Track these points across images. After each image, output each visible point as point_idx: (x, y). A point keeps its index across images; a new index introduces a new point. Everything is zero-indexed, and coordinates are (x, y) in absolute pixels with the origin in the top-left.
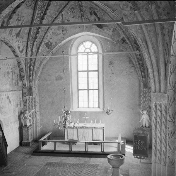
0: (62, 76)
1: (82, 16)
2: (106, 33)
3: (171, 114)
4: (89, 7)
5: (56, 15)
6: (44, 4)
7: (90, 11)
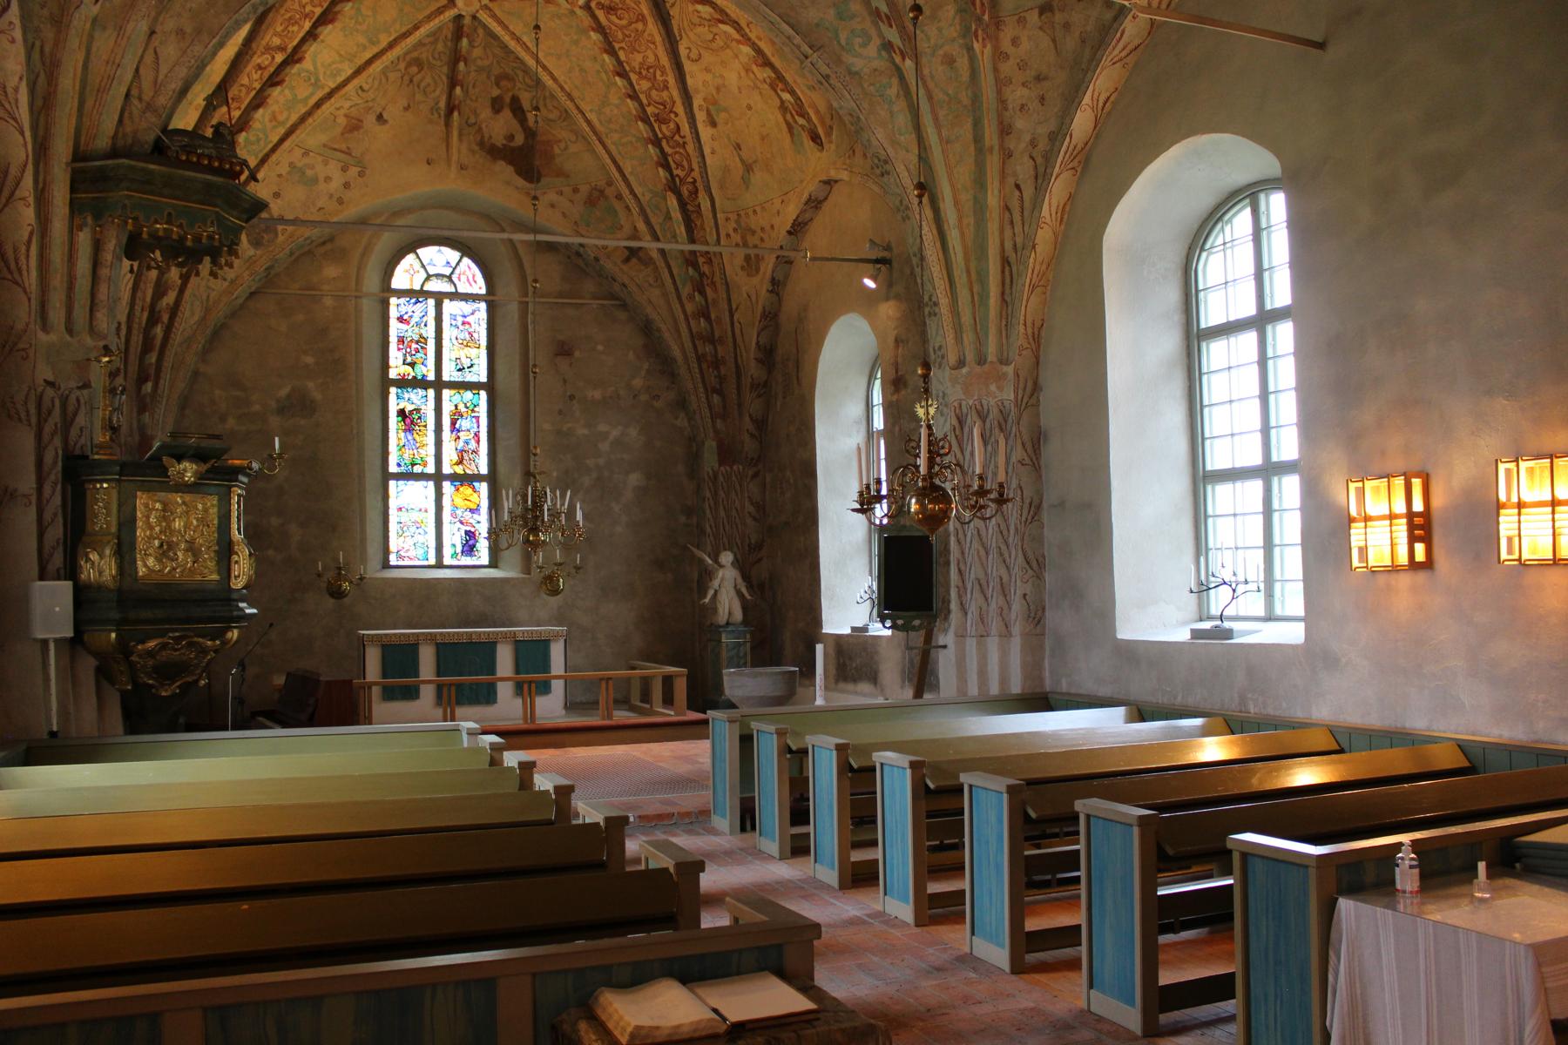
0: (318, 396)
1: (450, 109)
2: (553, 206)
3: (1026, 437)
4: (496, 71)
5: (340, 79)
6: (308, 8)
7: (496, 92)
